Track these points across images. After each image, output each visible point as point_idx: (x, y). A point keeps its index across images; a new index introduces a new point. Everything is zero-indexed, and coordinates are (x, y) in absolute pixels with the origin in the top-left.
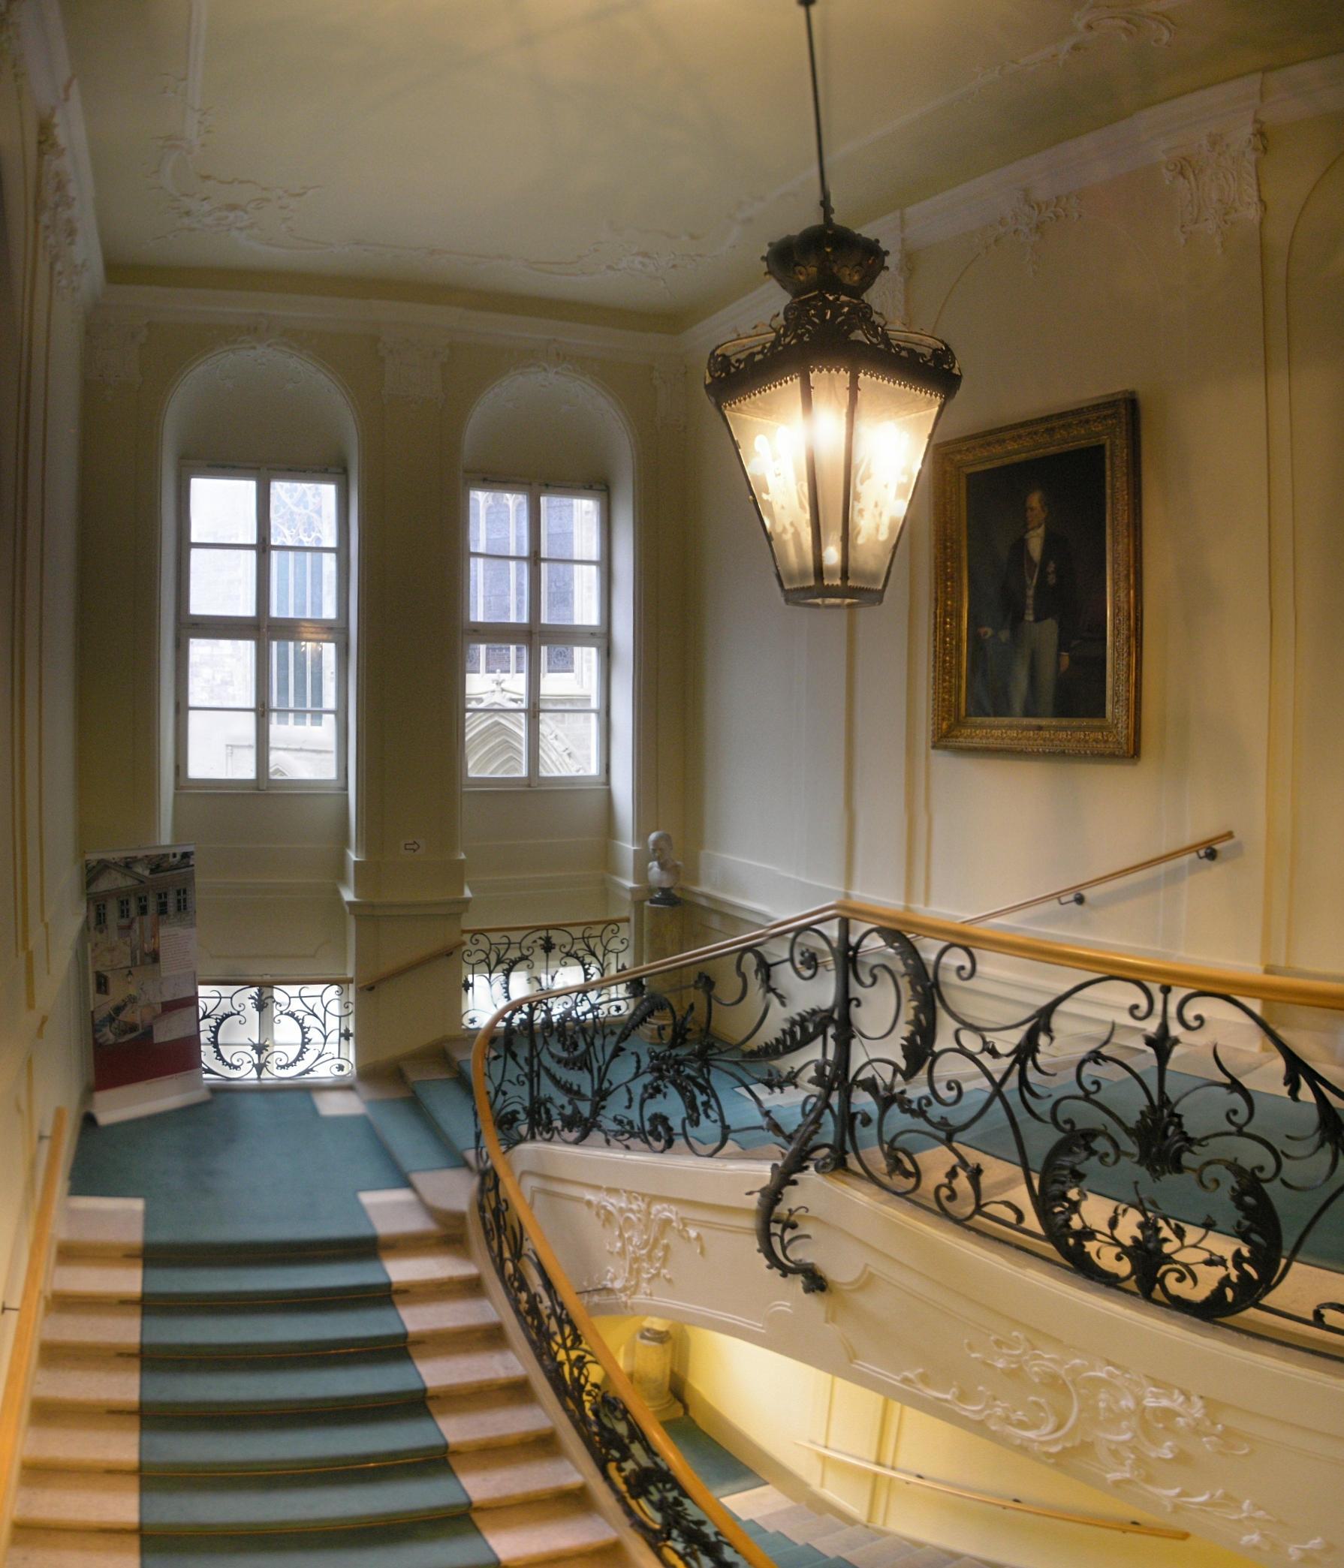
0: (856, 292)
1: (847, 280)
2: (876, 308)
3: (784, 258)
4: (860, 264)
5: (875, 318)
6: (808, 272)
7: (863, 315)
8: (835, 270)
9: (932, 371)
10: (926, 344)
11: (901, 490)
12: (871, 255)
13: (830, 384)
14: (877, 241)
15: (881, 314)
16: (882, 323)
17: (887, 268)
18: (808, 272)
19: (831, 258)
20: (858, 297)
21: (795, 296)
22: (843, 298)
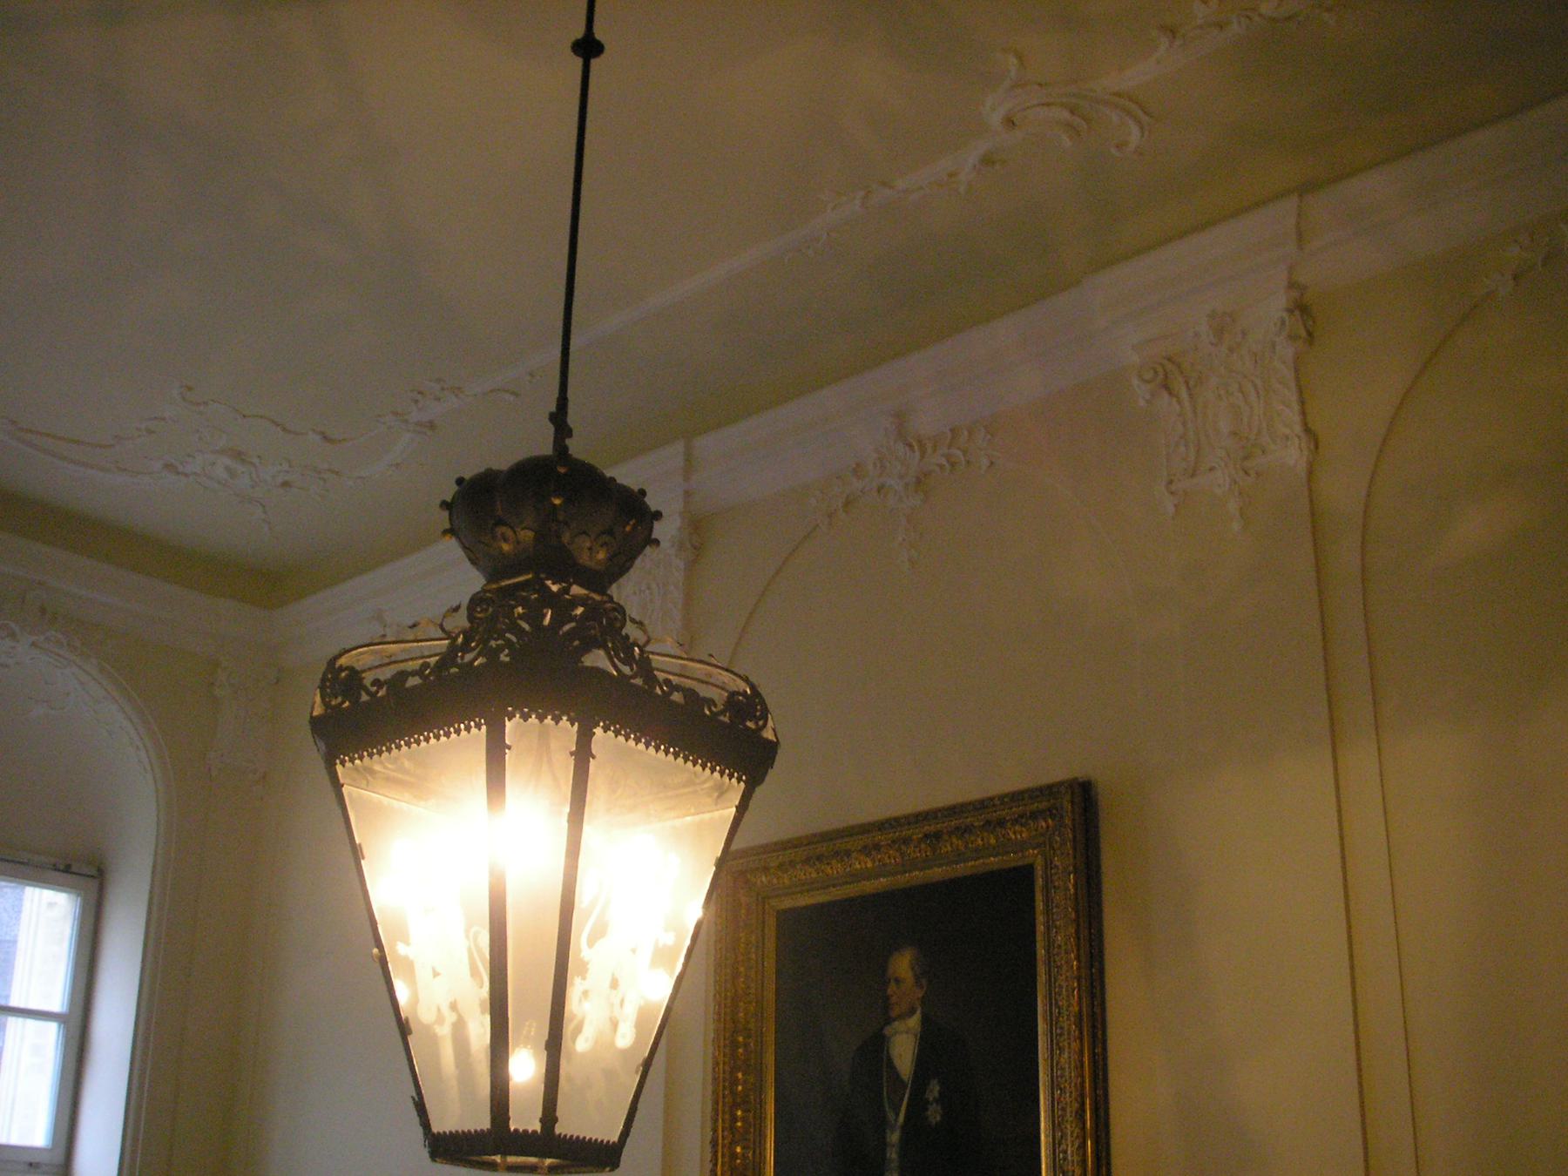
0: (600, 580)
1: (584, 559)
2: (633, 611)
3: (478, 504)
4: (610, 532)
5: (630, 630)
6: (517, 538)
7: (606, 625)
8: (566, 538)
9: (726, 737)
10: (717, 686)
11: (661, 956)
12: (634, 512)
13: (543, 743)
14: (643, 493)
15: (640, 624)
16: (642, 640)
17: (657, 542)
18: (517, 538)
20: (603, 592)
21: (492, 576)
22: (576, 590)
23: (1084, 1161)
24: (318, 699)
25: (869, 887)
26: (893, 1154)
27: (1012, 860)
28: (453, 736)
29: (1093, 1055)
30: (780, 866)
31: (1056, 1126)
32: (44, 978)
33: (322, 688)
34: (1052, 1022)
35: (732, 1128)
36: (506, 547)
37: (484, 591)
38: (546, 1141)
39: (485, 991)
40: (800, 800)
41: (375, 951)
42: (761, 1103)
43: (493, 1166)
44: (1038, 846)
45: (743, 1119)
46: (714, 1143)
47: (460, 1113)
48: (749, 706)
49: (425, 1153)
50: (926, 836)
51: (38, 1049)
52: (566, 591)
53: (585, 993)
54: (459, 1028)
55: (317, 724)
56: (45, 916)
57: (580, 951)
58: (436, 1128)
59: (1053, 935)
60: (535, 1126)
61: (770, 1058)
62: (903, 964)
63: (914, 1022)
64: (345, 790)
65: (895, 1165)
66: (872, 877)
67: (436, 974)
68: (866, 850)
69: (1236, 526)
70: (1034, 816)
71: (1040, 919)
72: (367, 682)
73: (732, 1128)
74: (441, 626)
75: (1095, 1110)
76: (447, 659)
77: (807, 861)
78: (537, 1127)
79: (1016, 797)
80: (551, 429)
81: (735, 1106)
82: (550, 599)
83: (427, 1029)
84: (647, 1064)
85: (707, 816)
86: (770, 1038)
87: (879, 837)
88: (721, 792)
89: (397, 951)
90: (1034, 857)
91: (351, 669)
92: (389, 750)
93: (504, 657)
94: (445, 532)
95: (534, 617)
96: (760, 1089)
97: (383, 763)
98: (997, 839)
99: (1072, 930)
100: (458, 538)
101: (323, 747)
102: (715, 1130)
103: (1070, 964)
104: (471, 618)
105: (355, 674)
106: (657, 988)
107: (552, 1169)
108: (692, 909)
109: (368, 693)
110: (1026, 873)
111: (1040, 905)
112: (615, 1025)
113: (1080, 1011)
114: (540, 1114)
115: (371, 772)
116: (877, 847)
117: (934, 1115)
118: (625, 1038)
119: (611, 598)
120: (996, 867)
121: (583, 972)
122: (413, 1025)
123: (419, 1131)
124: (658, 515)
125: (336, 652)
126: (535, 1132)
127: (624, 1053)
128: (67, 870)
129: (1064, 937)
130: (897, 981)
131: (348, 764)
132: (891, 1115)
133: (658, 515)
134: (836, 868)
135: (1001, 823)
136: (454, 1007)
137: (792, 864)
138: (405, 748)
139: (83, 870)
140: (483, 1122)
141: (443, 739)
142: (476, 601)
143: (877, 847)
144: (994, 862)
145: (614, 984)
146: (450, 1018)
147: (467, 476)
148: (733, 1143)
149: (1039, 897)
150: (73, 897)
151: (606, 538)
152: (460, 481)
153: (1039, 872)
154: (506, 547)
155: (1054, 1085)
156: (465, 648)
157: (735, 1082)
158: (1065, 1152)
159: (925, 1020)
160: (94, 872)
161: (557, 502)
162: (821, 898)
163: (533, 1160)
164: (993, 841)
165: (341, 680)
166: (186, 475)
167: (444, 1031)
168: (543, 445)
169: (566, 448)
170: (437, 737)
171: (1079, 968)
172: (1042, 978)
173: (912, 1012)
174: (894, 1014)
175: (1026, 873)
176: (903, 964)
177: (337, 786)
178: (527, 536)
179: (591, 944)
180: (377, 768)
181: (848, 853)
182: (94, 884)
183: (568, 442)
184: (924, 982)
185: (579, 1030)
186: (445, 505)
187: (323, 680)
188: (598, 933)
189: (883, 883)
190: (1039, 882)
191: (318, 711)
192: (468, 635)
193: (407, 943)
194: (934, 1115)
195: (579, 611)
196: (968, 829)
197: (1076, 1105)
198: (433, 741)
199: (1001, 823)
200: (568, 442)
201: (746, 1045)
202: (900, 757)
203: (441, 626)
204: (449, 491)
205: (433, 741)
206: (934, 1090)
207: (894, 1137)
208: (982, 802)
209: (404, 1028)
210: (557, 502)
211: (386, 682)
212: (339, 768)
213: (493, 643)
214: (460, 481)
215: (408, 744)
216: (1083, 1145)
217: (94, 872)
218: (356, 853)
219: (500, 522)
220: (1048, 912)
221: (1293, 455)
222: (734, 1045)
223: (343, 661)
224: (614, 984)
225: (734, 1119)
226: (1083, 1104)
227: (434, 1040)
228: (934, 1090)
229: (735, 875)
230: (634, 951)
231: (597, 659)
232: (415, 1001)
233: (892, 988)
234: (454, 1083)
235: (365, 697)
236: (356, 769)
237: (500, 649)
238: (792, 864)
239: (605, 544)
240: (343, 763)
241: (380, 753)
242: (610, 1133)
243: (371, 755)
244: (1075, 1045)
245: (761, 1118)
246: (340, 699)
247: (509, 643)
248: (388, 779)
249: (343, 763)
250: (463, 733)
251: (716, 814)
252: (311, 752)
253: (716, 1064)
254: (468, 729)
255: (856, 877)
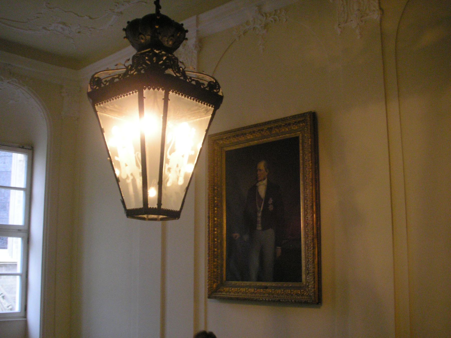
0: (171, 50)
1: (165, 44)
2: (181, 60)
3: (134, 29)
4: (173, 36)
5: (180, 65)
6: (146, 38)
7: (173, 63)
8: (160, 38)
9: (208, 94)
15: (182, 63)
16: (183, 67)
18: (146, 38)
19: (158, 31)
20: (171, 54)
21: (139, 51)
22: (163, 52)
23: (313, 221)
24: (89, 87)
25: (252, 143)
26: (259, 219)
27: (293, 135)
28: (129, 95)
29: (316, 190)
30: (226, 138)
31: (305, 210)
32: (18, 177)
33: (90, 84)
34: (304, 181)
35: (214, 213)
36: (143, 41)
37: (136, 54)
38: (159, 211)
39: (140, 170)
40: (231, 119)
41: (109, 158)
42: (222, 206)
43: (144, 219)
44: (300, 131)
45: (217, 210)
46: (209, 217)
47: (134, 203)
48: (214, 85)
49: (125, 215)
50: (268, 128)
51: (17, 200)
52: (161, 52)
53: (169, 169)
54: (134, 181)
55: (89, 94)
56: (18, 161)
57: (166, 156)
58: (128, 208)
59: (305, 157)
60: (156, 206)
61: (224, 193)
62: (262, 166)
63: (265, 182)
64: (98, 113)
65: (260, 222)
66: (253, 140)
67: (126, 165)
68: (250, 133)
69: (359, 38)
70: (299, 122)
71: (301, 152)
72: (103, 81)
73: (214, 213)
74: (124, 65)
75: (316, 206)
76: (125, 74)
77: (234, 137)
78: (156, 206)
79: (294, 117)
80: (154, 6)
81: (214, 207)
82: (156, 55)
83: (125, 180)
84: (187, 188)
85: (203, 118)
86: (224, 187)
87: (255, 129)
88: (207, 111)
89: (115, 159)
90: (299, 134)
91: (98, 78)
92: (110, 100)
93: (142, 72)
94: (125, 38)
95: (151, 60)
96: (221, 201)
97: (108, 105)
98: (288, 129)
99: (310, 155)
100: (129, 39)
101: (91, 100)
102: (209, 213)
103: (309, 164)
104: (133, 62)
105: (99, 80)
106: (189, 169)
107: (162, 219)
108: (199, 146)
109: (104, 84)
110: (297, 138)
111: (301, 148)
112: (178, 179)
113: (312, 178)
114: (157, 203)
115: (105, 108)
116: (254, 132)
117: (271, 208)
118: (181, 182)
119: (174, 56)
120: (288, 137)
121: (168, 162)
122: (120, 179)
123: (123, 209)
124: (187, 31)
125: (94, 73)
126: (155, 208)
127: (181, 186)
128: (23, 147)
129: (308, 157)
130: (260, 170)
131: (99, 105)
132: (258, 209)
133: (187, 31)
134: (242, 138)
135: (289, 124)
136: (132, 174)
137: (230, 137)
138: (115, 100)
139: (28, 148)
140: (141, 206)
141: (126, 96)
142: (134, 57)
143: (254, 132)
144: (288, 136)
145: (177, 166)
146: (131, 178)
147: (130, 21)
148: (214, 217)
149: (300, 145)
150: (25, 155)
151: (172, 38)
152: (128, 22)
153: (300, 138)
154: (143, 41)
155: (305, 199)
156: (131, 70)
157: (214, 200)
158: (308, 218)
159: (268, 181)
160: (30, 148)
161: (157, 27)
162: (237, 147)
163: (155, 216)
164: (287, 130)
165: (96, 81)
166: (49, 30)
167: (129, 181)
168: (152, 10)
169: (159, 11)
170: (124, 96)
171: (312, 166)
172: (301, 169)
173: (264, 179)
174: (259, 180)
175: (297, 138)
176: (262, 166)
177: (96, 112)
178: (148, 37)
179: (170, 154)
180: (108, 107)
181: (245, 134)
182: (31, 151)
183: (160, 10)
184: (268, 170)
185: (168, 181)
186: (124, 30)
187: (91, 81)
188: (173, 151)
189: (256, 142)
190: (301, 141)
191: (89, 90)
192: (132, 66)
193: (118, 156)
194: (271, 208)
195: (164, 58)
196: (280, 126)
197: (311, 204)
198: (123, 97)
199: (289, 124)
200: (160, 10)
201: (217, 190)
202: (260, 105)
203: (124, 65)
204: (125, 25)
205: (123, 97)
206: (271, 201)
207: (260, 214)
208: (284, 118)
209: (118, 180)
210: (157, 27)
211: (109, 81)
212: (96, 107)
213: (139, 68)
214: (128, 22)
215: (116, 98)
216: (313, 215)
217: (30, 148)
218: (102, 131)
219: (140, 34)
220: (303, 149)
221: (376, 16)
222: (214, 190)
223: (96, 76)
224: (177, 166)
225: (214, 210)
226: (313, 204)
227: (127, 185)
228: (271, 201)
229: (213, 141)
230: (183, 156)
231: (170, 71)
232: (121, 172)
233: (259, 172)
234: (133, 197)
235: (103, 86)
236: (101, 107)
237: (141, 69)
238: (230, 137)
239: (171, 40)
240: (97, 105)
241: (108, 101)
242: (178, 209)
243: (105, 102)
244: (311, 188)
245: (222, 210)
246: (95, 87)
247: (144, 68)
248: (111, 110)
249: (97, 105)
250: (132, 94)
251: (206, 118)
252: (88, 102)
253: (209, 195)
254: (133, 93)
255: (248, 141)
